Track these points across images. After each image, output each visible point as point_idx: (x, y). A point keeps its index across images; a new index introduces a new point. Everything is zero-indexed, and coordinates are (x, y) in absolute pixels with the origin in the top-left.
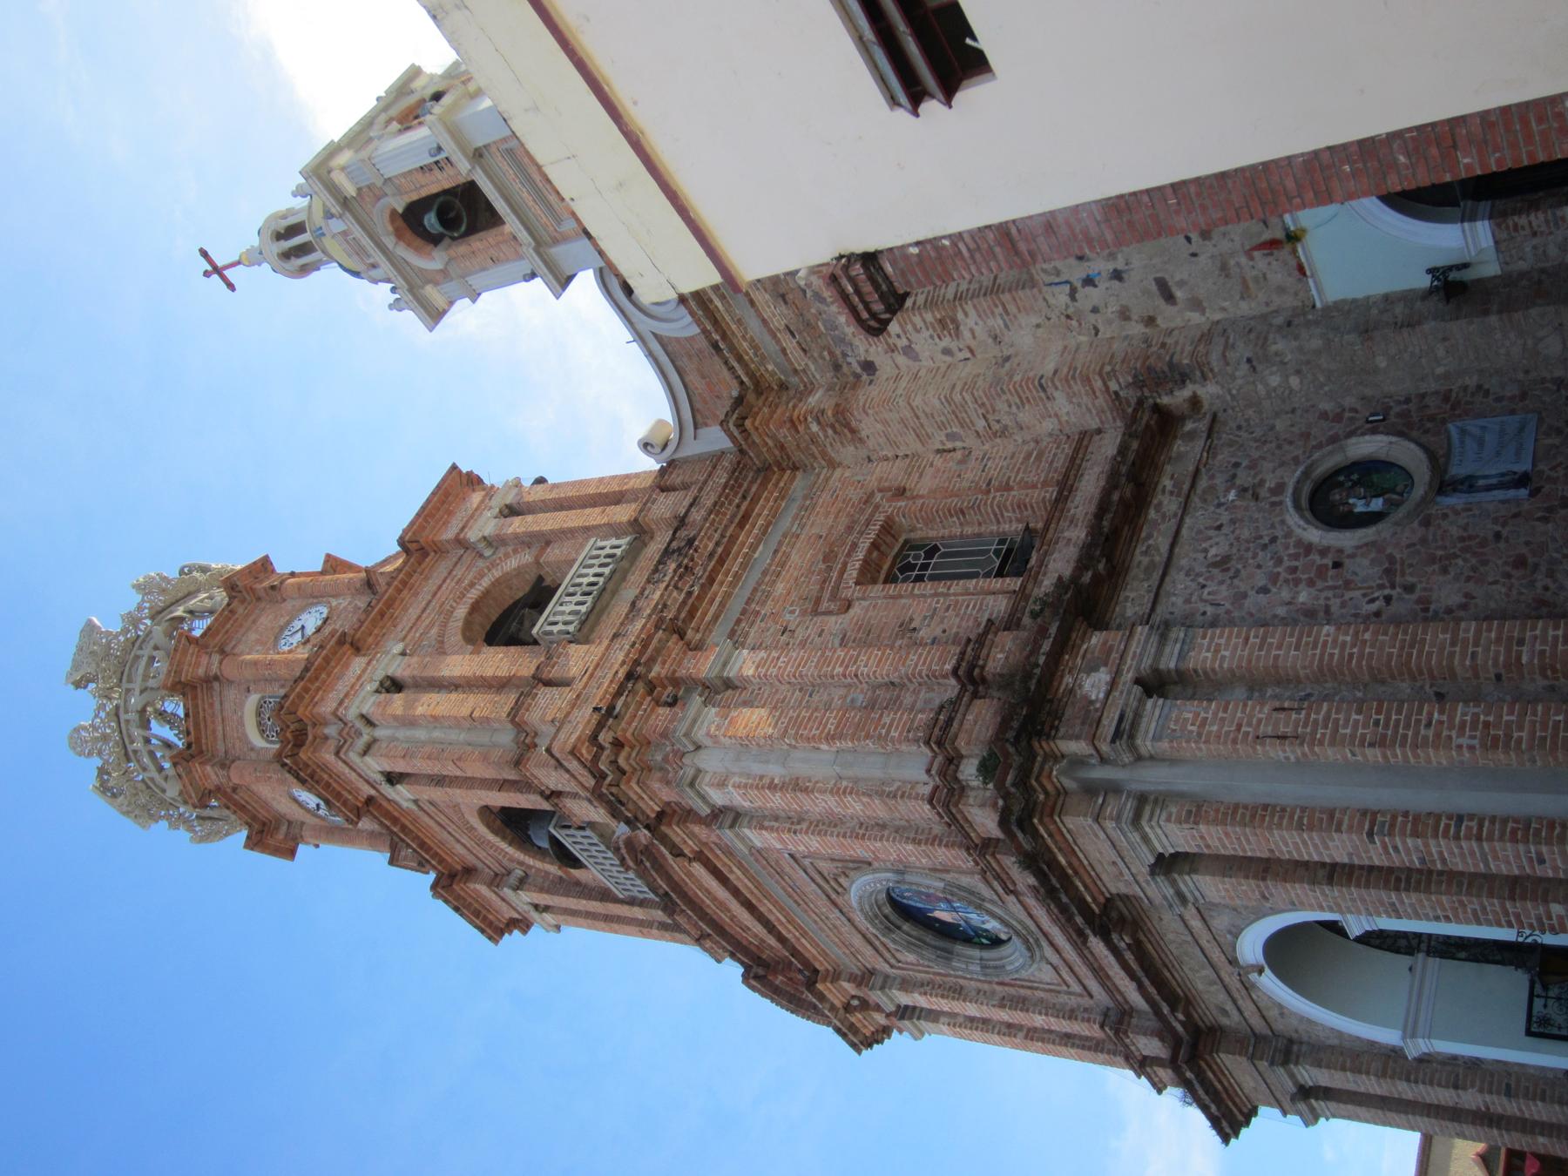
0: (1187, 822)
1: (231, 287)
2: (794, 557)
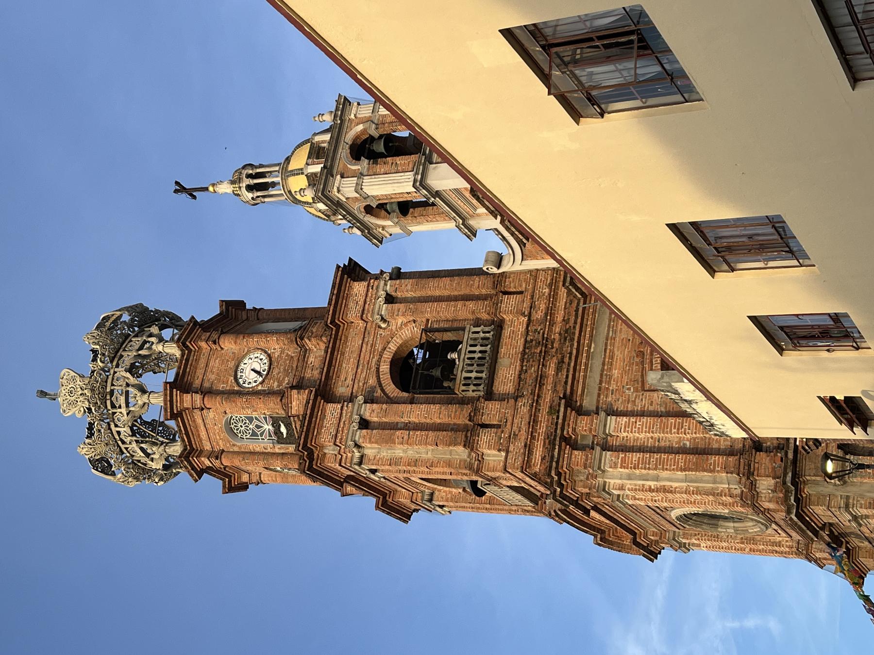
1: (194, 197)
2: (617, 353)
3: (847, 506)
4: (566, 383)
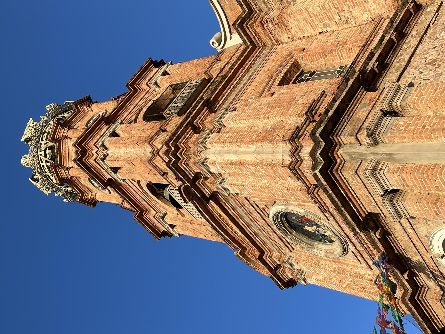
0: (397, 172)
3: (374, 169)
4: (213, 93)
